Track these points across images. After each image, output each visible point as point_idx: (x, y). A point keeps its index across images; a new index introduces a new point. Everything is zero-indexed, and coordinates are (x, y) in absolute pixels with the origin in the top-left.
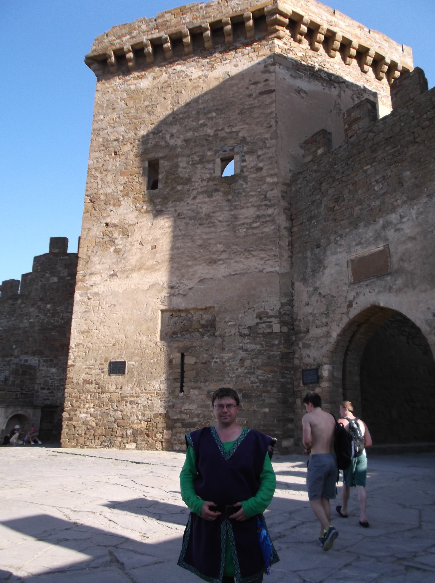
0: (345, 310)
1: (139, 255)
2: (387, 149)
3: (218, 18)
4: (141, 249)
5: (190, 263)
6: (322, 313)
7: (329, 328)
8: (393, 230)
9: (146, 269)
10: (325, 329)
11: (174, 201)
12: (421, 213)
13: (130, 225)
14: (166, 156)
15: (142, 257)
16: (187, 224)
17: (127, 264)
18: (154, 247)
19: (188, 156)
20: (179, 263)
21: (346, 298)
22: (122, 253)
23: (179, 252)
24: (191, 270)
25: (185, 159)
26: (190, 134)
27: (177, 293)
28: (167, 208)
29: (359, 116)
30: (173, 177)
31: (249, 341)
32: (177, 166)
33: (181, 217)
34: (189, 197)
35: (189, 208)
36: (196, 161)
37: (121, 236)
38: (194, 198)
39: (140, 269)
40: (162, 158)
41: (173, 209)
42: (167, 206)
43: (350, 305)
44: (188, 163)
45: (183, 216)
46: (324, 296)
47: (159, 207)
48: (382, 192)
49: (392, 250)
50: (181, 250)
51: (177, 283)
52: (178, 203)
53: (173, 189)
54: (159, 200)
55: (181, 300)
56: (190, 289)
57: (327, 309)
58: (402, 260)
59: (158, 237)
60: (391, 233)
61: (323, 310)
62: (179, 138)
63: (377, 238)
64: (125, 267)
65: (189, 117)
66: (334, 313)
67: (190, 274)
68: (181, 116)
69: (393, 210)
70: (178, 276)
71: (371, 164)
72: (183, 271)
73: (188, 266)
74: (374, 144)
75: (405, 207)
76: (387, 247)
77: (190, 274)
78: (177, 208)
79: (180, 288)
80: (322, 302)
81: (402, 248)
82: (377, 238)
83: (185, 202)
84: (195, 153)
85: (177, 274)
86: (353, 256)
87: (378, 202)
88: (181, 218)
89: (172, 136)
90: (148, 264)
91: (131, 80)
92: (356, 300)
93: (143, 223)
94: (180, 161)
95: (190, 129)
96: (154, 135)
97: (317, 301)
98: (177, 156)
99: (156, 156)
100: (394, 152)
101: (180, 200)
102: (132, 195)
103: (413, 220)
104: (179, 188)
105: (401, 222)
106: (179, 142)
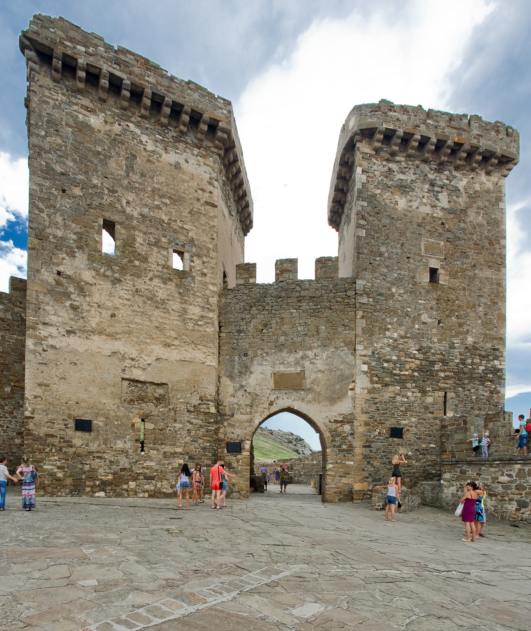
0: (267, 406)
1: (97, 320)
2: (311, 304)
3: (180, 100)
4: (101, 313)
5: (148, 341)
6: (247, 405)
7: (252, 416)
8: (309, 362)
9: (106, 335)
10: (248, 417)
11: (132, 275)
12: (330, 357)
13: (87, 283)
14: (122, 223)
15: (101, 322)
16: (145, 303)
17: (87, 325)
18: (113, 316)
19: (145, 233)
20: (138, 338)
21: (268, 398)
22: (79, 310)
23: (138, 327)
24: (148, 347)
25: (142, 235)
26: (146, 211)
27: (137, 365)
28: (126, 280)
29: (290, 269)
30: (130, 249)
31: (193, 417)
32: (134, 240)
33: (139, 293)
34: (147, 277)
35: (146, 287)
36: (152, 242)
37: (77, 292)
38: (151, 279)
39: (100, 333)
40: (118, 222)
41: (131, 283)
42: (126, 277)
43: (271, 404)
44: (144, 240)
45: (140, 294)
46: (249, 393)
47: (117, 275)
48: (304, 333)
49: (307, 374)
50: (140, 326)
51: (137, 357)
52: (136, 279)
53: (131, 261)
54: (117, 268)
55: (141, 373)
56: (149, 364)
57: (252, 403)
58: (313, 383)
59: (119, 306)
60: (307, 364)
61: (249, 402)
62: (136, 209)
63: (297, 363)
64: (84, 327)
65: (144, 190)
66: (257, 407)
67: (148, 351)
68: (137, 185)
69: (311, 349)
70: (137, 350)
71: (297, 309)
72: (142, 346)
73: (146, 343)
74: (300, 296)
75: (319, 349)
76: (303, 372)
77: (148, 351)
78: (136, 283)
79: (139, 362)
80: (247, 397)
81: (313, 376)
82: (297, 363)
83: (143, 280)
84: (151, 233)
85: (137, 348)
86: (277, 369)
87: (300, 339)
88: (139, 295)
89: (128, 203)
90: (108, 330)
91: (76, 104)
92: (276, 402)
93: (101, 286)
94: (137, 235)
95: (145, 205)
96: (108, 192)
97: (243, 395)
98: (134, 228)
99: (112, 218)
100: (316, 309)
101: (139, 277)
102: (86, 250)
103: (324, 360)
104: (137, 263)
105: (315, 359)
106: (136, 214)
